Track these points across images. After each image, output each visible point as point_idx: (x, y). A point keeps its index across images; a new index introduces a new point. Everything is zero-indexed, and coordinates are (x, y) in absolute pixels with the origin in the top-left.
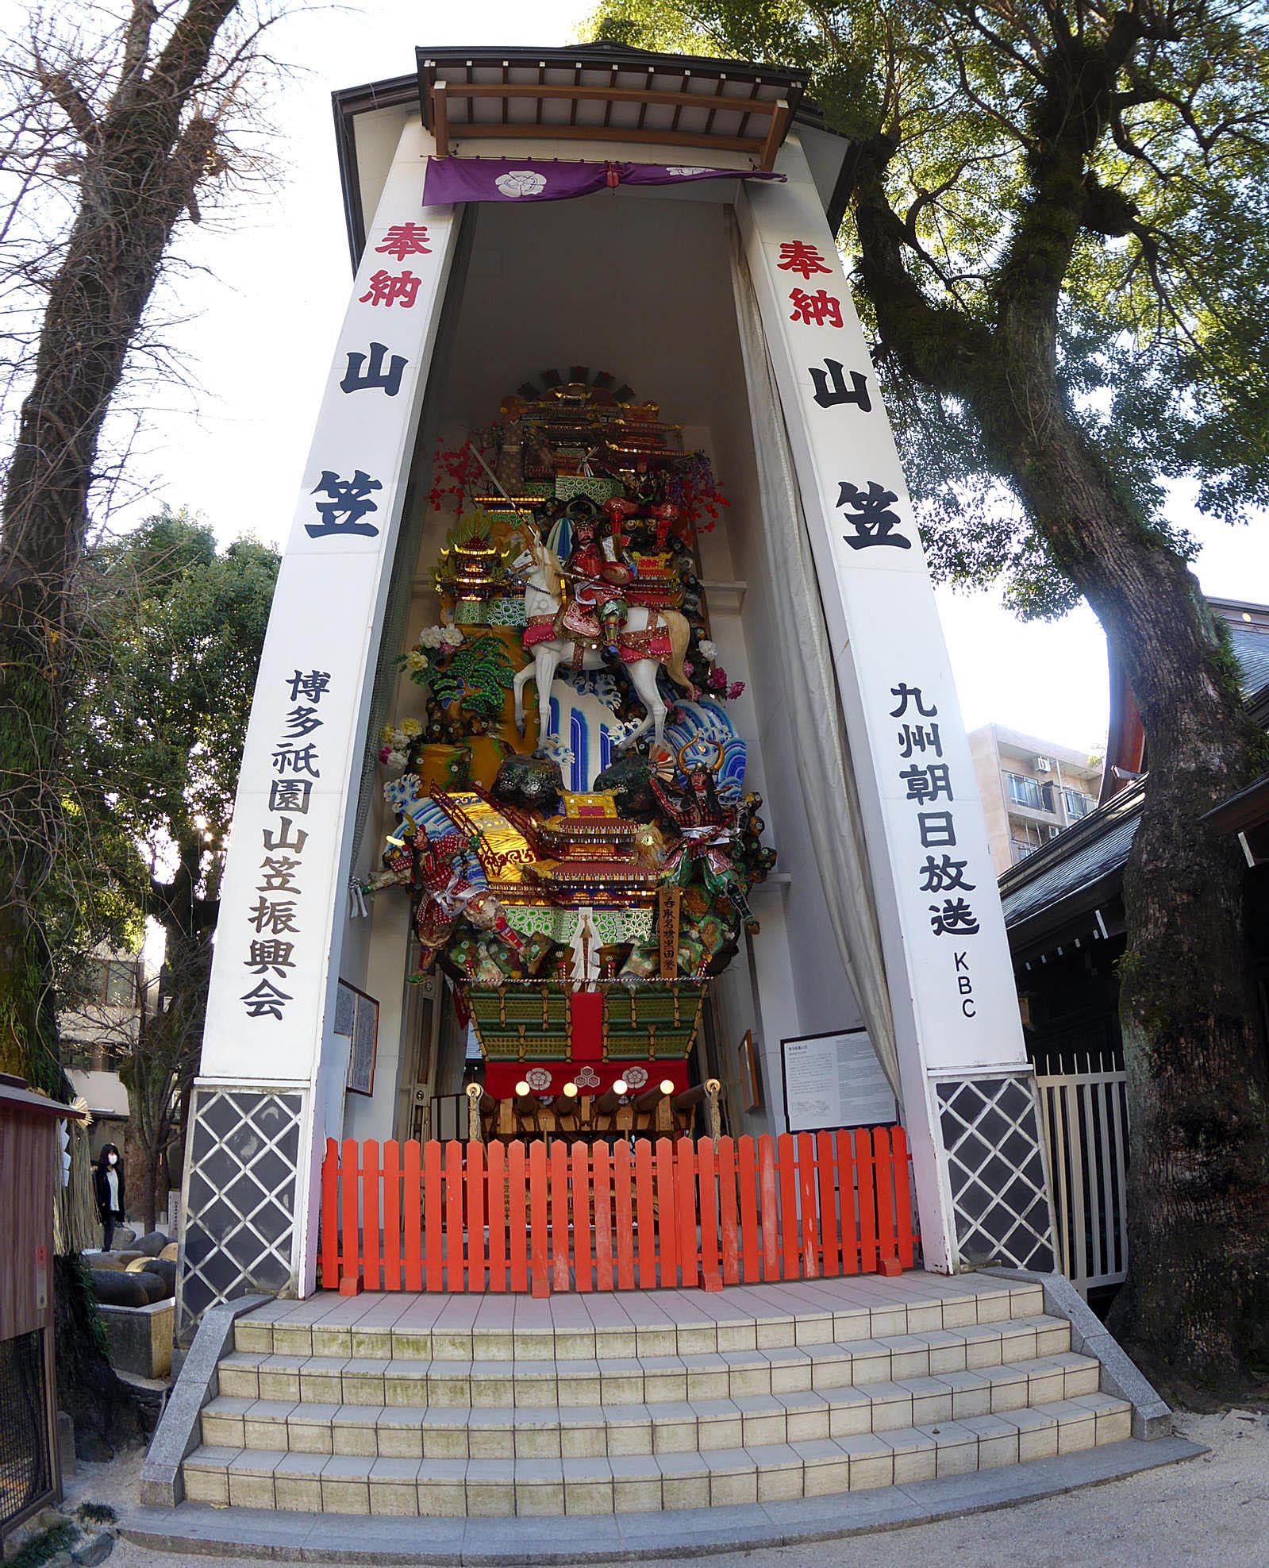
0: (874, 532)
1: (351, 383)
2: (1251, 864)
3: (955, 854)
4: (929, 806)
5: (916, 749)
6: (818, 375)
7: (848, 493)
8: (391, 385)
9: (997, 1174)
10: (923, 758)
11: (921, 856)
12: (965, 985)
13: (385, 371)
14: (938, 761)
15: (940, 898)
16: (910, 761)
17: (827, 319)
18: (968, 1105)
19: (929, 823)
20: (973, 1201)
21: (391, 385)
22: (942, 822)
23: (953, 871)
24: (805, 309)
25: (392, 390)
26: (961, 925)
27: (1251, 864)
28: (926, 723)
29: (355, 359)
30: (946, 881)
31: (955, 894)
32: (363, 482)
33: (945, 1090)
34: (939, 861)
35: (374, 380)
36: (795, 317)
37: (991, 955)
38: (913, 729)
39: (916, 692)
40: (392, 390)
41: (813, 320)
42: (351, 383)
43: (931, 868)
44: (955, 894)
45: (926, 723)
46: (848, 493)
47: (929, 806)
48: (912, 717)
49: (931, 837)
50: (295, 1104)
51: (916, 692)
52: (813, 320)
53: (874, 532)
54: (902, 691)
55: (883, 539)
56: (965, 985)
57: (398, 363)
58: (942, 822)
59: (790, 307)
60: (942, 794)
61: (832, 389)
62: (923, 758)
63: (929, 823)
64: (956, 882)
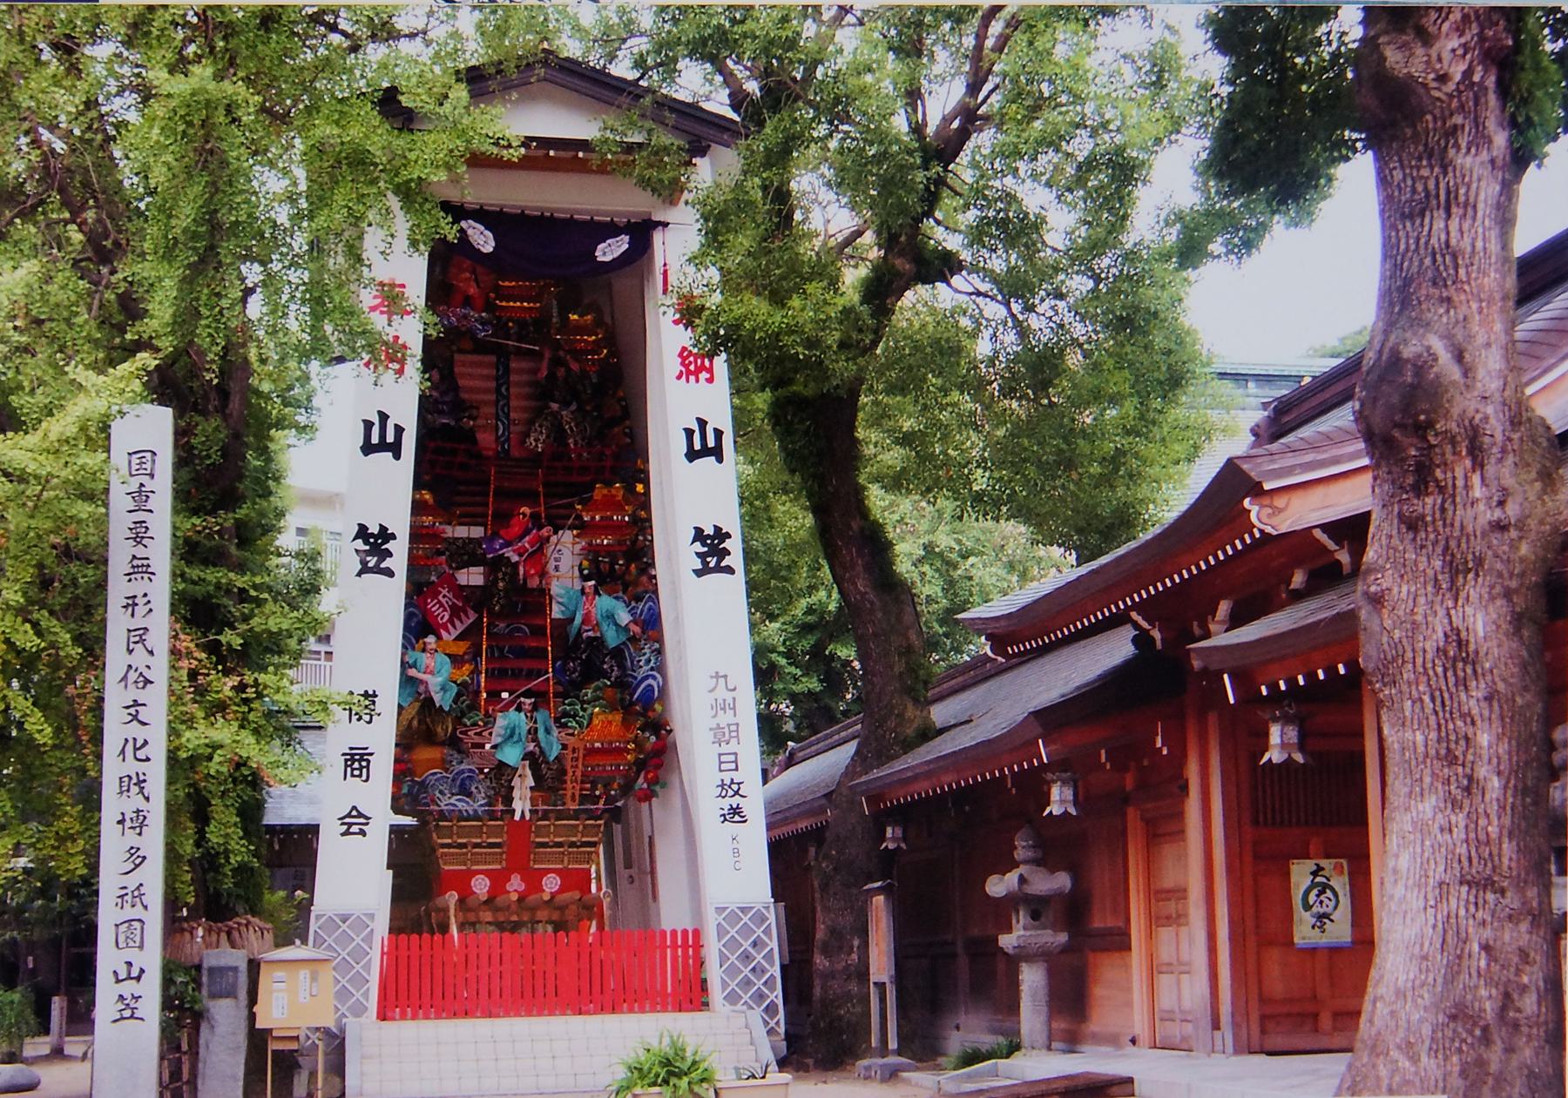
0: (712, 565)
1: (368, 449)
2: (1232, 701)
3: (737, 777)
4: (725, 748)
5: (721, 713)
6: (689, 433)
7: (699, 535)
8: (395, 448)
9: (746, 957)
10: (725, 718)
11: (717, 778)
12: (736, 852)
13: (390, 438)
14: (733, 720)
15: (726, 803)
16: (716, 721)
17: (704, 375)
18: (733, 918)
19: (724, 758)
20: (732, 971)
21: (395, 448)
22: (732, 758)
23: (735, 787)
24: (687, 366)
25: (397, 456)
26: (737, 818)
27: (1232, 701)
28: (729, 696)
29: (368, 425)
30: (731, 793)
31: (735, 801)
32: (385, 535)
33: (720, 910)
34: (728, 782)
35: (383, 446)
36: (679, 377)
37: (755, 839)
38: (720, 701)
39: (725, 677)
40: (397, 456)
41: (692, 378)
42: (368, 449)
43: (722, 785)
44: (735, 801)
45: (729, 696)
46: (699, 535)
47: (725, 748)
48: (721, 693)
49: (724, 766)
50: (372, 916)
51: (725, 677)
52: (692, 378)
53: (712, 565)
54: (717, 676)
55: (719, 569)
56: (736, 852)
57: (399, 430)
58: (732, 758)
59: (674, 366)
60: (733, 741)
61: (697, 446)
62: (725, 718)
63: (724, 758)
64: (737, 793)
